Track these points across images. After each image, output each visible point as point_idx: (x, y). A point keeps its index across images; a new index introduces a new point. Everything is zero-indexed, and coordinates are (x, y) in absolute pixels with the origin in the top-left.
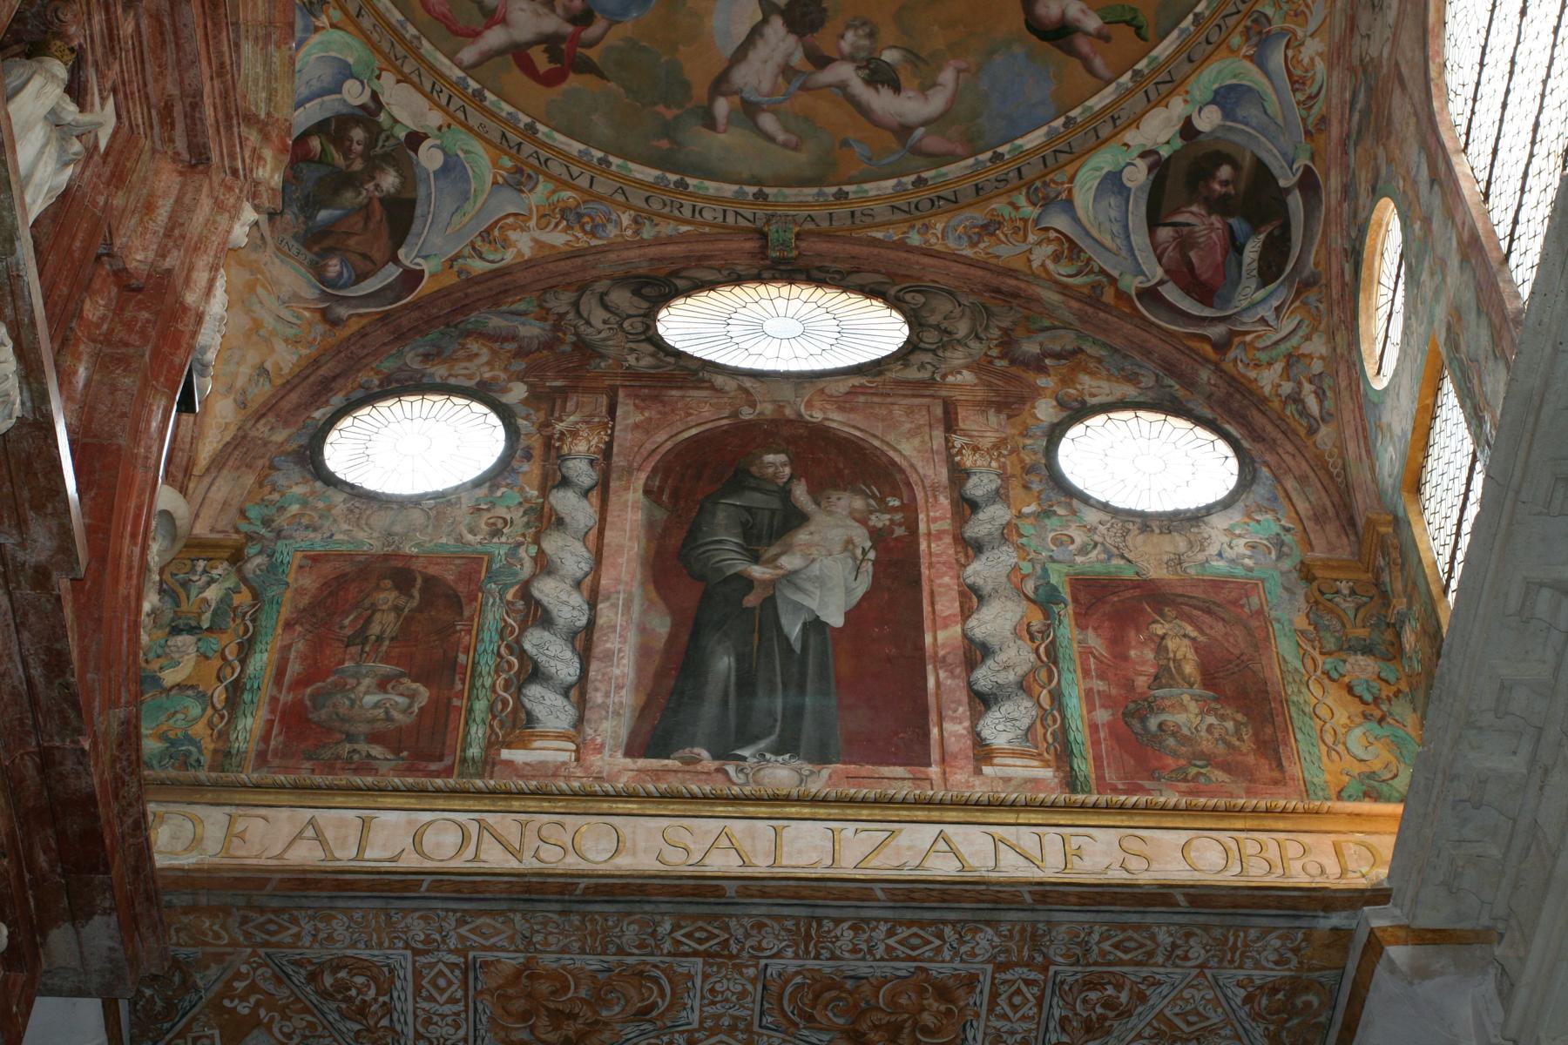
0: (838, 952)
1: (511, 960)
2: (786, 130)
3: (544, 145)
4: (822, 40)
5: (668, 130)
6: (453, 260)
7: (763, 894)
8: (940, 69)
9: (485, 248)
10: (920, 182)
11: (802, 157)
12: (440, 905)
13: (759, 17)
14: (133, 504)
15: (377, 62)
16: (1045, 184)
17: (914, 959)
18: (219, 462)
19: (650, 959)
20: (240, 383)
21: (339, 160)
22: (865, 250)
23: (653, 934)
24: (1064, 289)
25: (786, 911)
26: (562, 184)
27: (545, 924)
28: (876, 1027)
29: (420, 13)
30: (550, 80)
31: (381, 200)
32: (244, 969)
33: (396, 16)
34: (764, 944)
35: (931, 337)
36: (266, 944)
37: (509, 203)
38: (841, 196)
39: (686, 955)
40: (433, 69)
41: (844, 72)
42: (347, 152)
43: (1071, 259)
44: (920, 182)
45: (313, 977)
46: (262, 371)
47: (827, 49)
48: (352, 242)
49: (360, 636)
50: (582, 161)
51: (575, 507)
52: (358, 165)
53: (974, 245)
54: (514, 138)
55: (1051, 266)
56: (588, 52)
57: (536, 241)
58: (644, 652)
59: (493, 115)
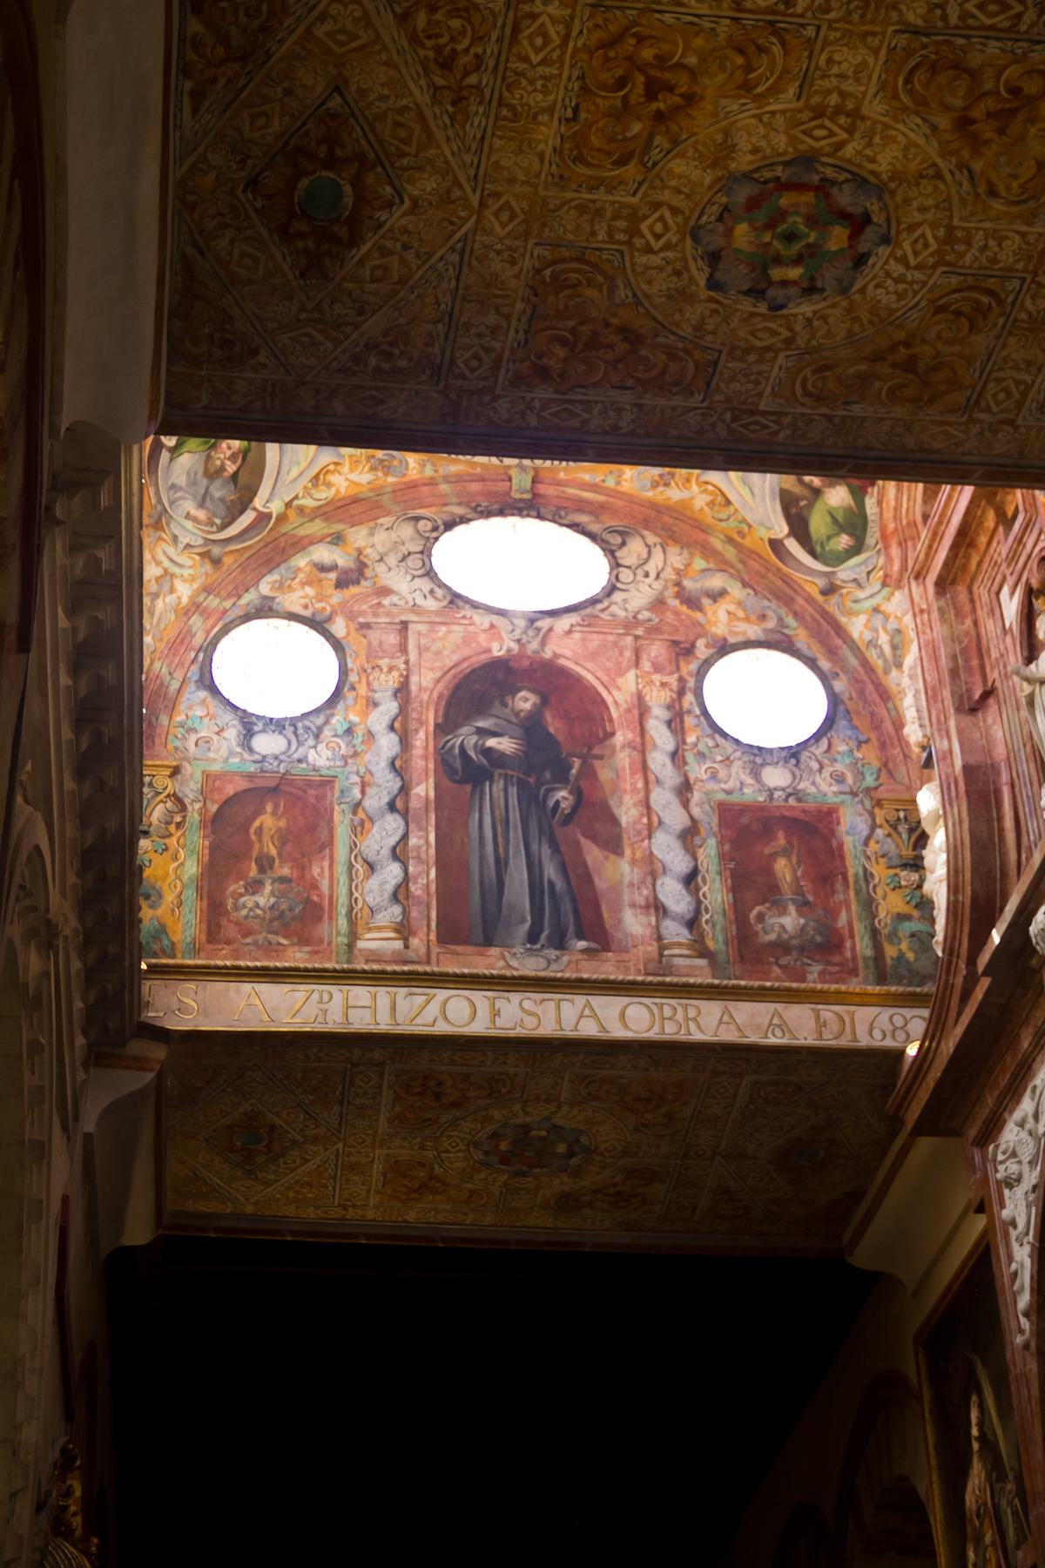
0: (635, 409)
17: (567, 401)
19: (805, 410)
28: (611, 346)
34: (700, 418)
39: (772, 413)
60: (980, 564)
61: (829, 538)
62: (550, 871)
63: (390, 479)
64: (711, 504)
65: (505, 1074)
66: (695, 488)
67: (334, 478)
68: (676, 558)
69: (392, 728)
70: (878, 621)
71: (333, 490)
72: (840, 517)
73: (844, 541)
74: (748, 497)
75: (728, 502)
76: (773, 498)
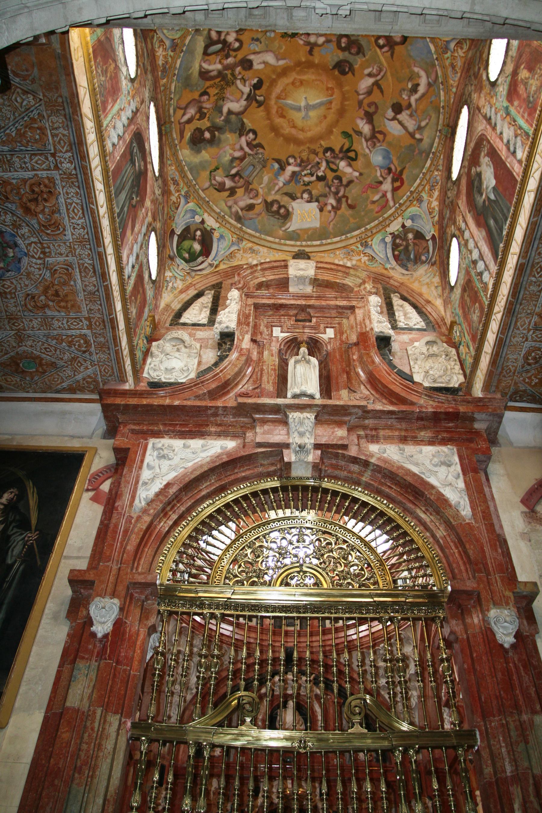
1: (535, 319)
2: (426, 119)
3: (415, 190)
4: (404, 104)
5: (421, 153)
6: (433, 225)
7: (527, 252)
8: (414, 71)
9: (433, 215)
10: (442, 83)
11: (433, 116)
12: (510, 334)
13: (396, 121)
14: (384, 372)
15: (383, 231)
16: (442, 48)
18: (445, 312)
20: (436, 295)
21: (402, 248)
22: (454, 107)
23: (535, 282)
24: (469, 49)
25: (535, 246)
26: (423, 189)
27: (524, 309)
29: (380, 214)
30: (402, 183)
31: (414, 239)
32: (521, 379)
33: (376, 222)
35: (469, 101)
36: (514, 373)
37: (425, 205)
38: (443, 107)
40: (390, 216)
41: (413, 99)
42: (401, 245)
43: (462, 44)
44: (442, 83)
45: (529, 364)
46: (436, 287)
47: (407, 103)
48: (420, 251)
49: (468, 309)
50: (421, 181)
51: (467, 235)
52: (404, 243)
53: (457, 73)
54: (411, 198)
55: (464, 51)
56: (398, 170)
57: (436, 200)
58: (486, 242)
59: (405, 202)
60: (273, 315)
61: (184, 250)
62: (126, 209)
63: (160, 73)
64: (174, 203)
65: (64, 230)
66: (177, 194)
67: (161, 49)
68: (160, 198)
69: (132, 112)
70: (174, 280)
71: (157, 50)
72: (192, 250)
73: (187, 256)
74: (182, 216)
75: (177, 209)
76: (186, 224)
